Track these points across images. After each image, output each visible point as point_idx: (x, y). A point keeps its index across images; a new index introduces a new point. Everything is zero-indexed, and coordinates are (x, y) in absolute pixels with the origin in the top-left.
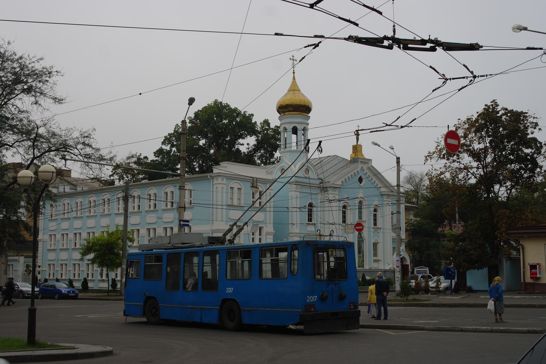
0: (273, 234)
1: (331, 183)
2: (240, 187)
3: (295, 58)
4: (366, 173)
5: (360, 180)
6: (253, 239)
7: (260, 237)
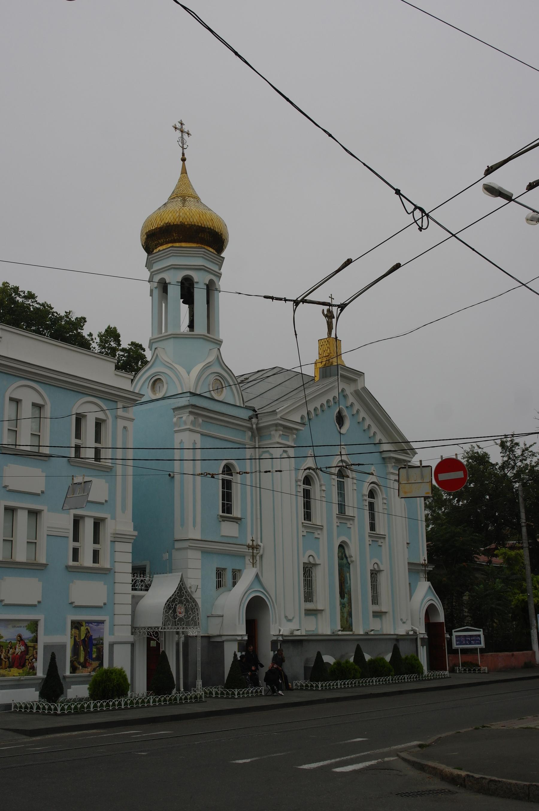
0: (132, 541)
1: (279, 416)
2: (40, 402)
3: (185, 128)
4: (352, 404)
5: (340, 420)
6: (76, 551)
7: (97, 546)
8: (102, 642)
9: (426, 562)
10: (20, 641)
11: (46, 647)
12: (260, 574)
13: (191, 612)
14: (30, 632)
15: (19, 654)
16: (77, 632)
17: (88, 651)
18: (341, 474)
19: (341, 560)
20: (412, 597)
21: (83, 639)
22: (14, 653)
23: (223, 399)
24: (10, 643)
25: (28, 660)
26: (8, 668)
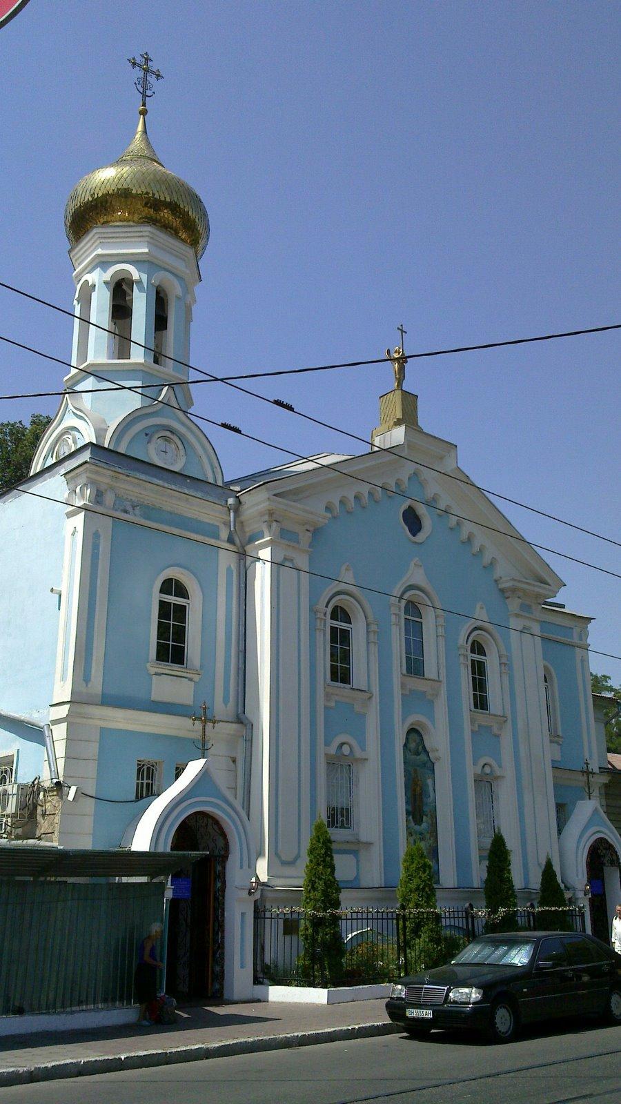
3: (154, 66)
18: (413, 608)
19: (415, 755)
20: (566, 828)
23: (181, 470)
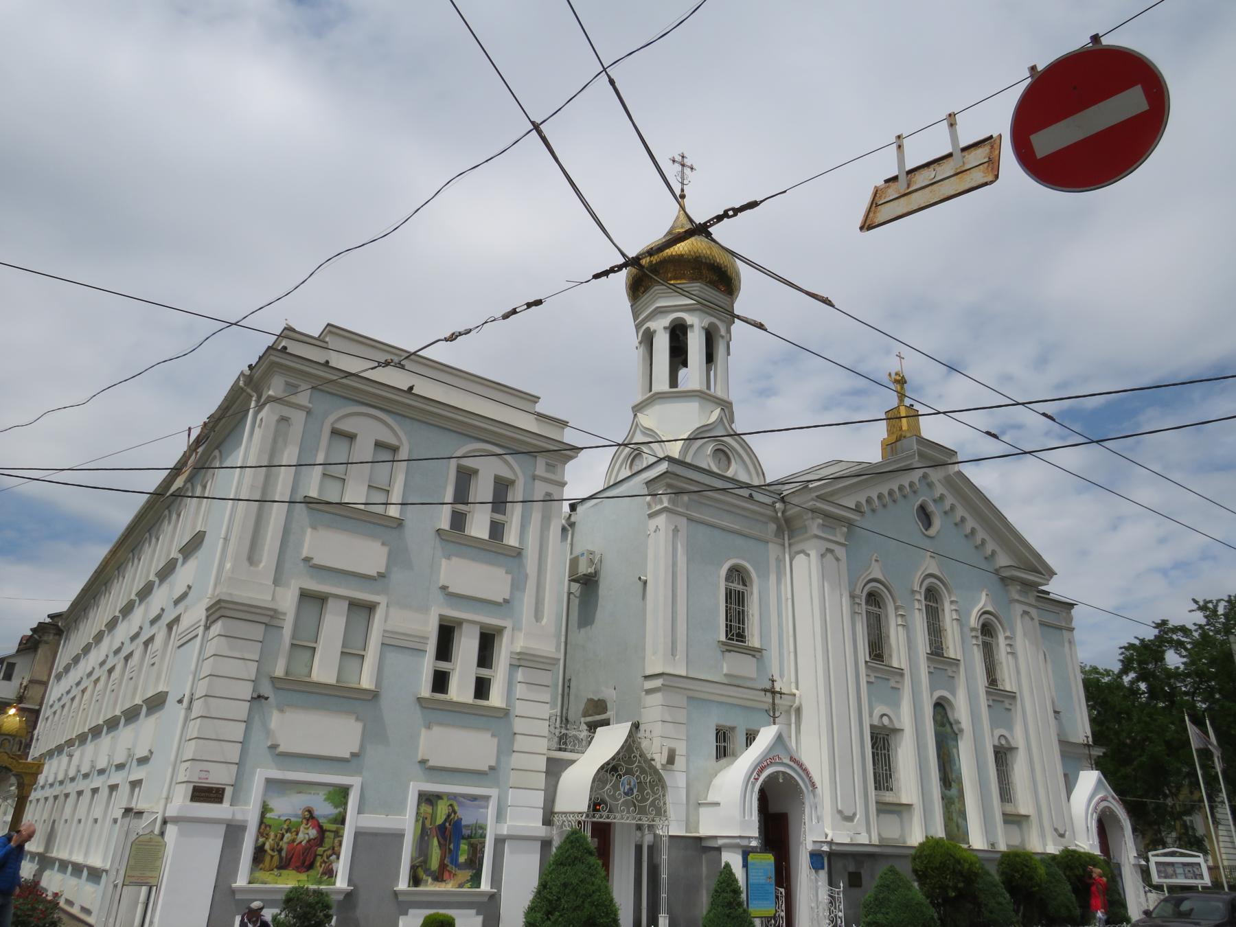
2: (392, 441)
3: (688, 162)
5: (925, 516)
8: (483, 832)
9: (1090, 739)
10: (308, 820)
11: (359, 835)
12: (785, 735)
13: (650, 791)
14: (330, 804)
15: (303, 843)
16: (429, 810)
17: (449, 849)
18: (932, 595)
21: (440, 825)
22: (294, 841)
24: (288, 822)
25: (322, 856)
26: (275, 870)
